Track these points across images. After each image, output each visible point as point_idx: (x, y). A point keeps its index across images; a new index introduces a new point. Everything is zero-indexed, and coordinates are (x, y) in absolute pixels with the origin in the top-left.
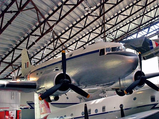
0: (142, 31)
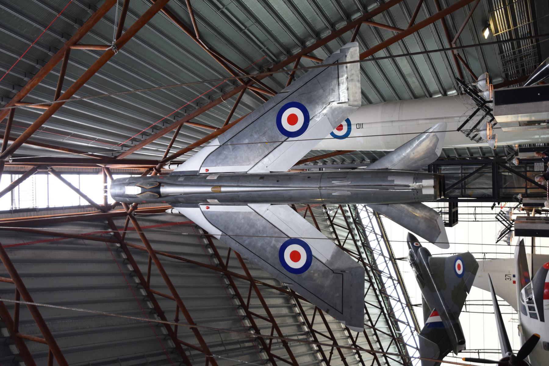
0: (403, 335)
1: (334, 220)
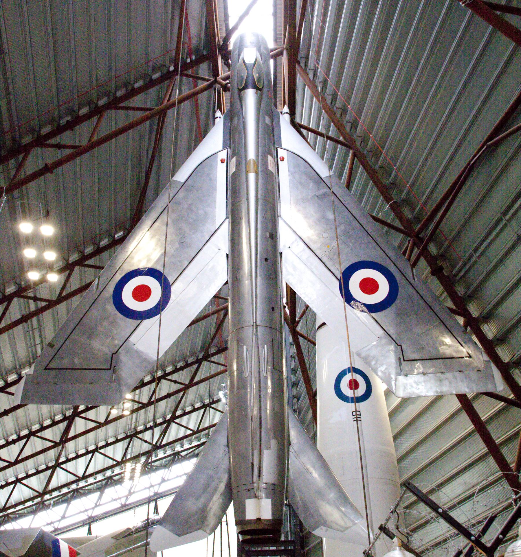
1: (211, 409)
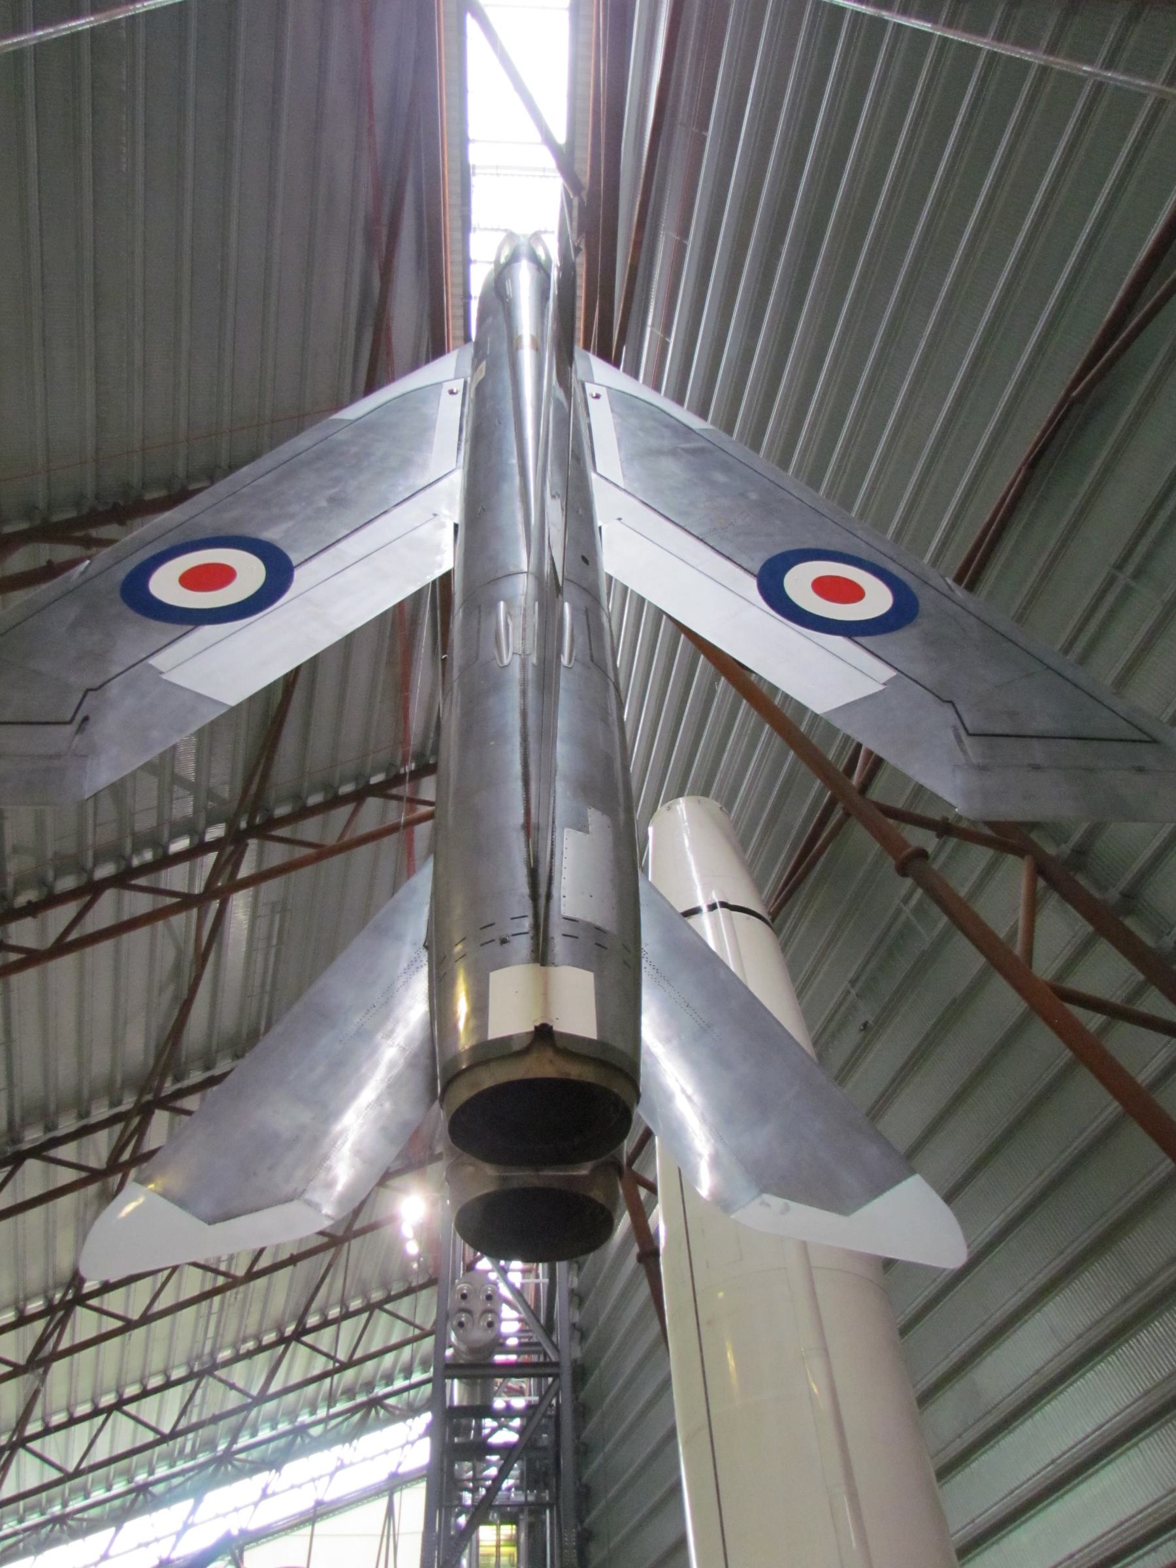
1: (384, 1315)
